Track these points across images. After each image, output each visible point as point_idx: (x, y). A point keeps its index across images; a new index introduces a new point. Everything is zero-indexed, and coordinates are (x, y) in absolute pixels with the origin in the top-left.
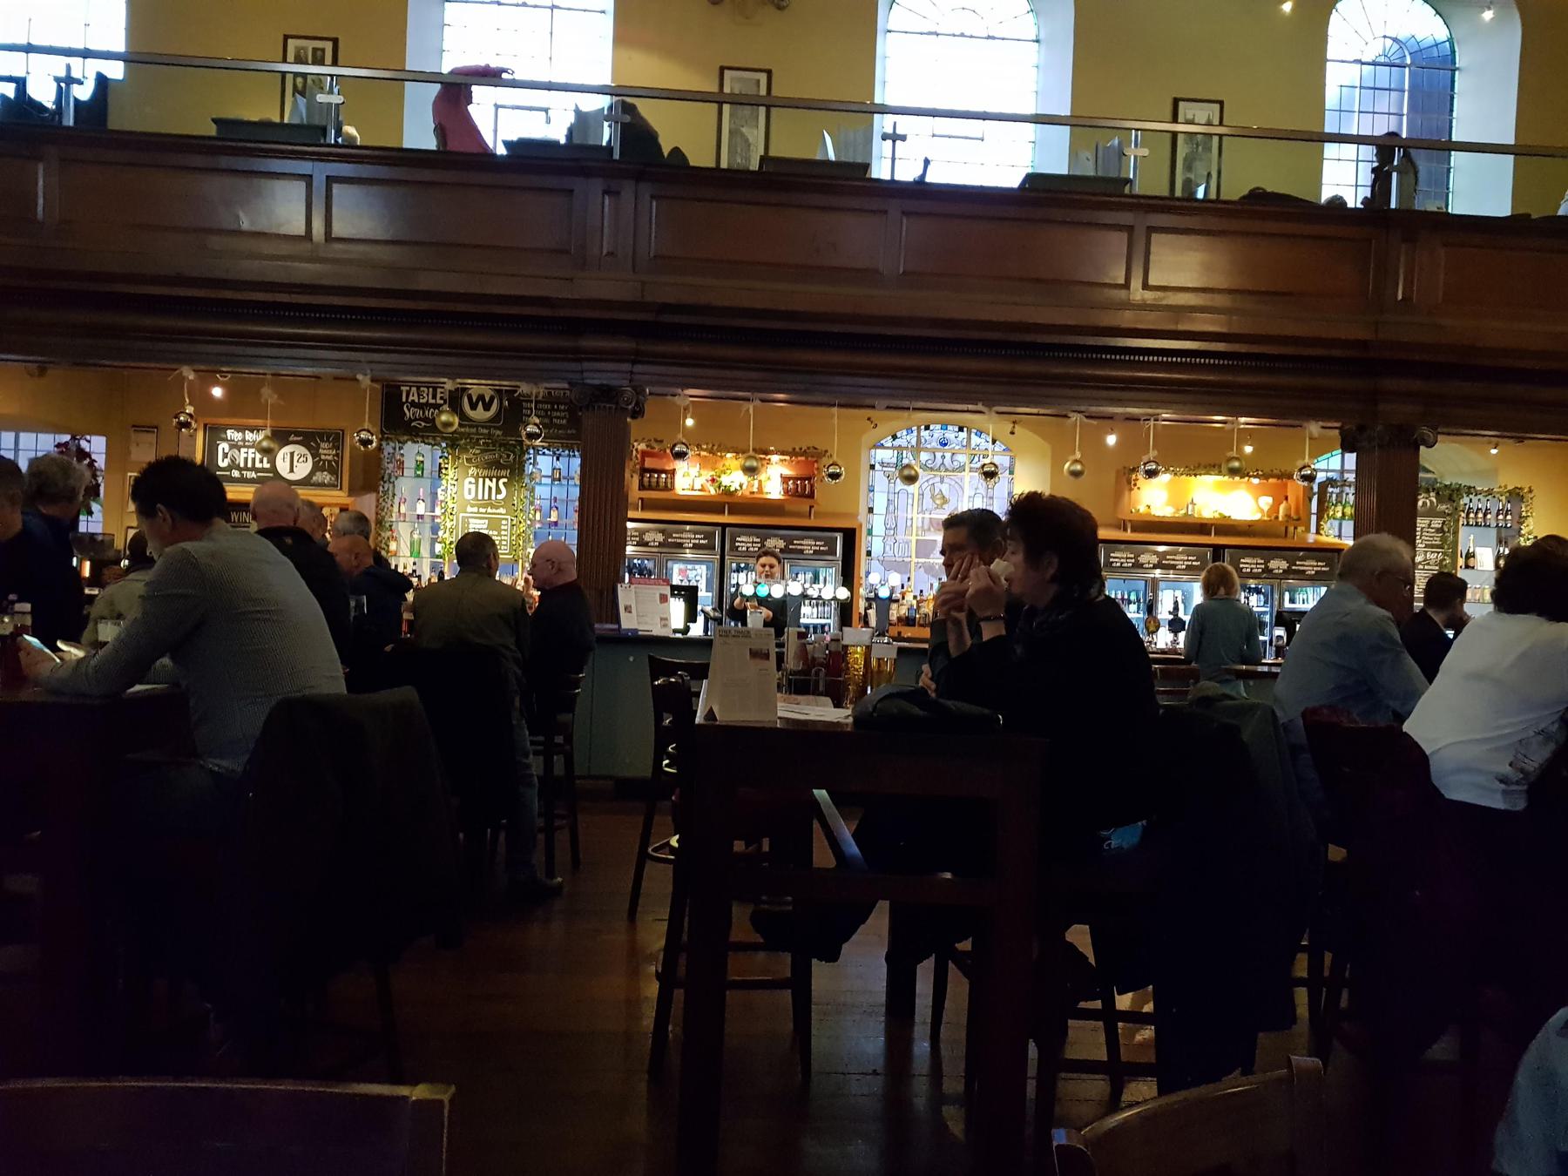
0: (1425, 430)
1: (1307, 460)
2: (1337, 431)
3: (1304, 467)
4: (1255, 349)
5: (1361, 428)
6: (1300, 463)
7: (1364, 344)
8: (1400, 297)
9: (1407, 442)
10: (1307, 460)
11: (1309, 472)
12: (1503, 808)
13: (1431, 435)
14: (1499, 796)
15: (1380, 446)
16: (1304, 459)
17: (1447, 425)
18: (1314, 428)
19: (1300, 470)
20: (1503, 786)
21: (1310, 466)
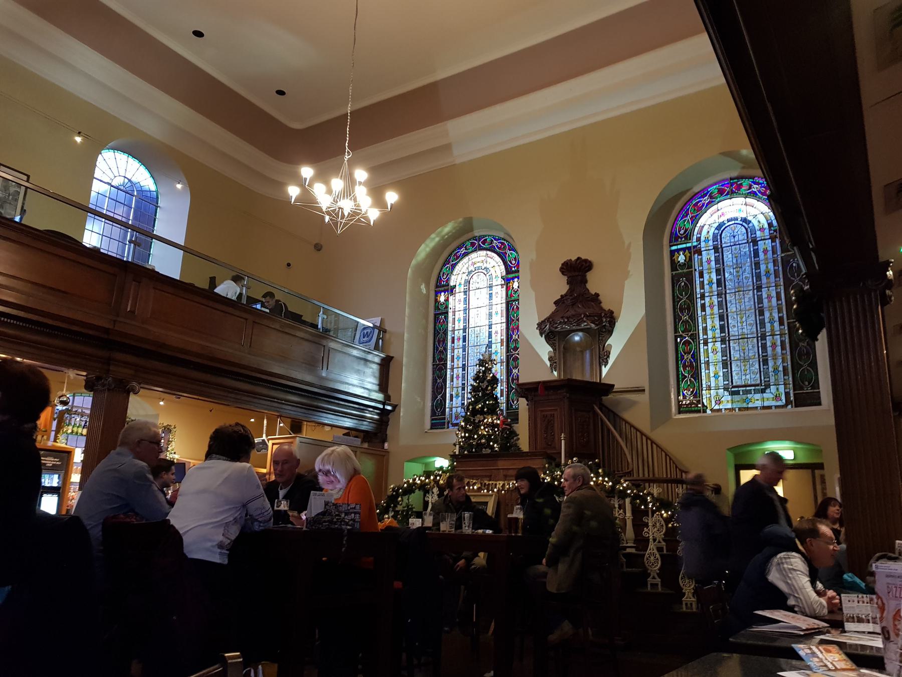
0: (134, 384)
1: (64, 392)
2: (85, 378)
3: (62, 396)
4: (41, 319)
5: (99, 378)
6: (60, 393)
7: (107, 331)
8: (128, 310)
9: (124, 390)
10: (64, 392)
11: (65, 399)
12: (218, 561)
13: (137, 387)
14: (218, 556)
15: (109, 390)
16: (63, 390)
17: (147, 383)
18: (72, 374)
19: (60, 397)
20: (219, 550)
21: (66, 396)
